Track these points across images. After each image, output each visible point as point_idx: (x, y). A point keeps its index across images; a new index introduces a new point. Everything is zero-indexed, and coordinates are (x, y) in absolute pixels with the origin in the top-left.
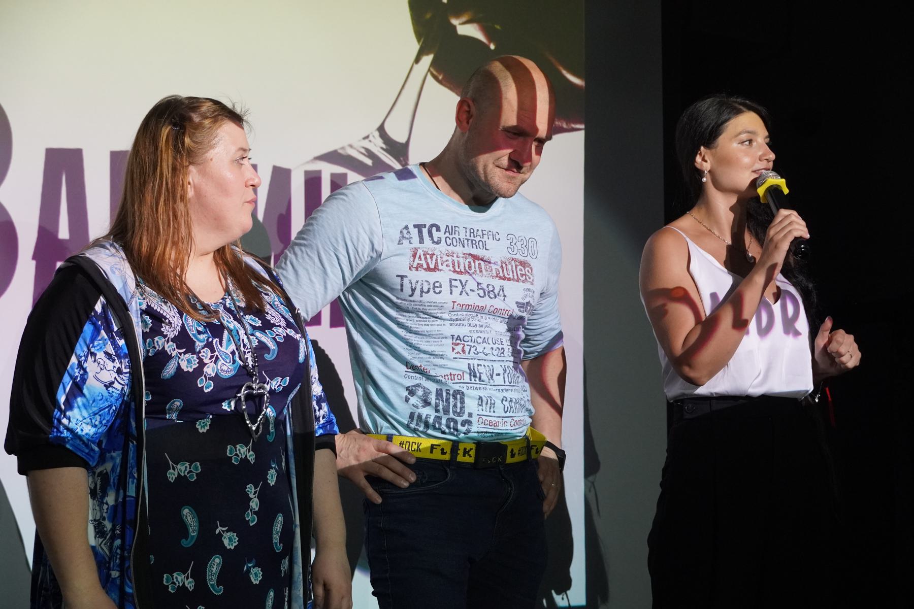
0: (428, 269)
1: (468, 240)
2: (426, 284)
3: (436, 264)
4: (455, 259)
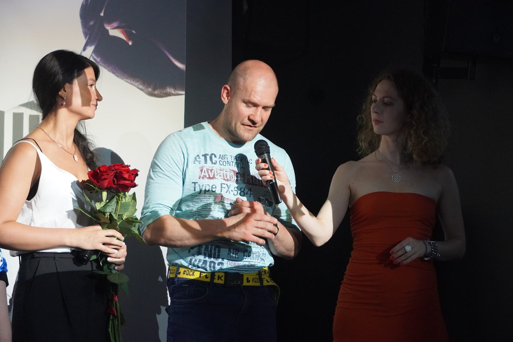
0: (210, 178)
1: (233, 162)
2: (207, 186)
3: (214, 175)
4: (225, 173)
